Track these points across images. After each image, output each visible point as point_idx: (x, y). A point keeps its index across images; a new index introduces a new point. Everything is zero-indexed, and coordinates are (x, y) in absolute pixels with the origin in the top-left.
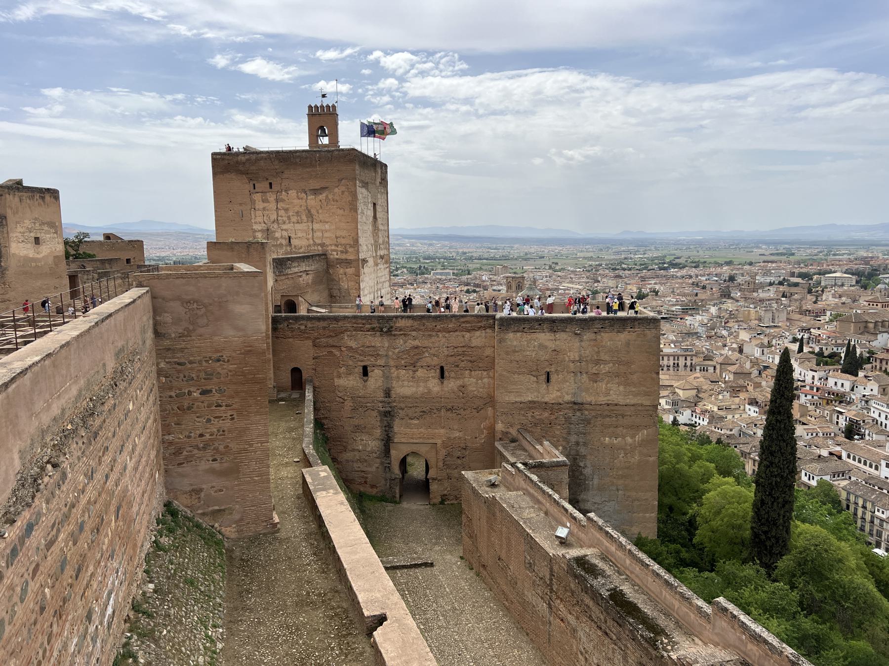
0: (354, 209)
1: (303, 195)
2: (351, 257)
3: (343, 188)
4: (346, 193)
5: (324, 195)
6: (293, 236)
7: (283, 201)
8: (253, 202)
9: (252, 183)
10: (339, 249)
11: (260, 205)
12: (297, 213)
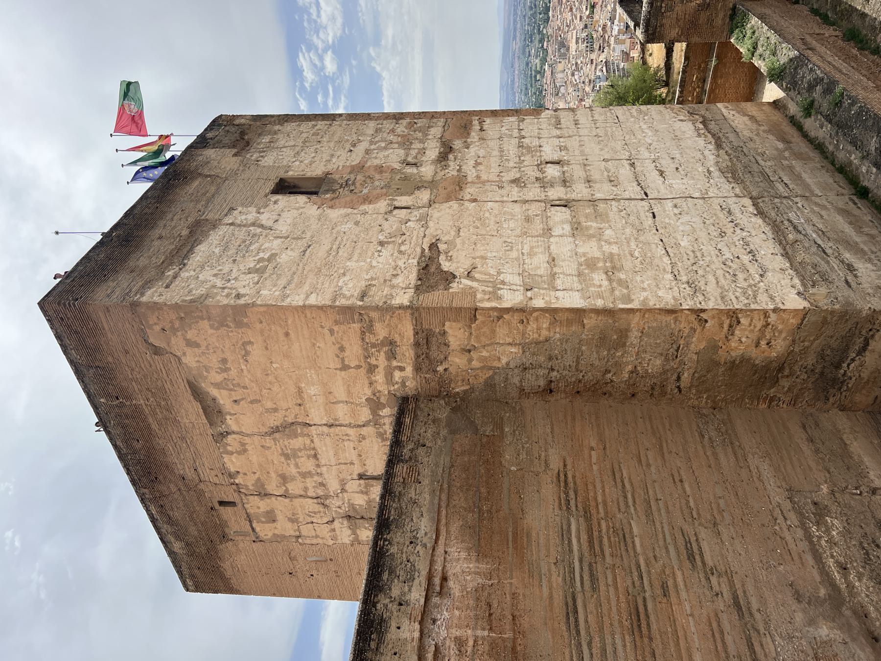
0: (238, 315)
2: (407, 330)
4: (190, 335)
5: (214, 392)
6: (357, 469)
7: (259, 483)
8: (279, 539)
10: (381, 360)
11: (284, 527)
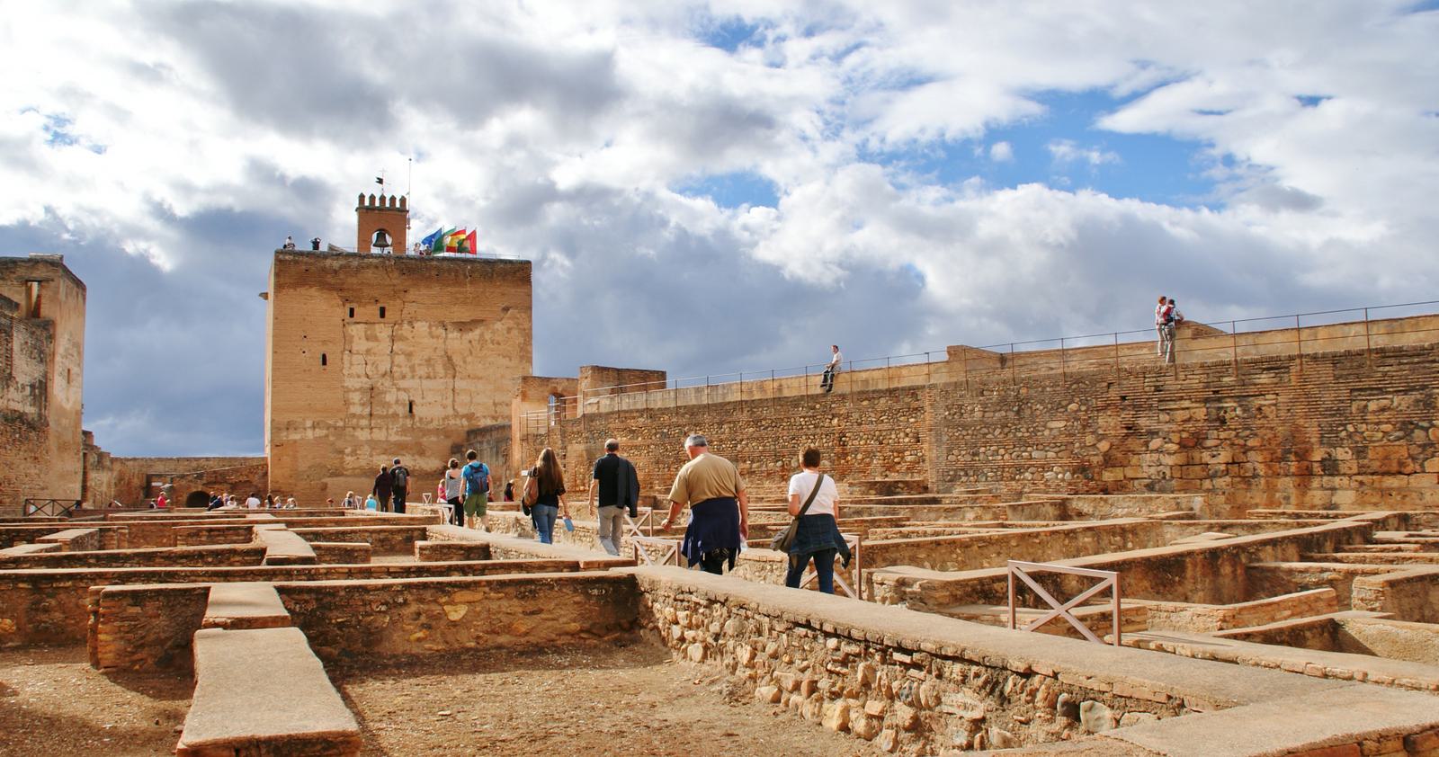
1: (441, 331)
3: (511, 323)
4: (515, 332)
6: (418, 400)
7: (403, 339)
8: (347, 339)
9: (348, 306)
11: (360, 345)
12: (428, 360)
